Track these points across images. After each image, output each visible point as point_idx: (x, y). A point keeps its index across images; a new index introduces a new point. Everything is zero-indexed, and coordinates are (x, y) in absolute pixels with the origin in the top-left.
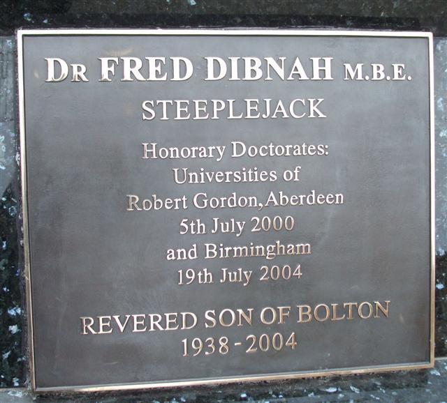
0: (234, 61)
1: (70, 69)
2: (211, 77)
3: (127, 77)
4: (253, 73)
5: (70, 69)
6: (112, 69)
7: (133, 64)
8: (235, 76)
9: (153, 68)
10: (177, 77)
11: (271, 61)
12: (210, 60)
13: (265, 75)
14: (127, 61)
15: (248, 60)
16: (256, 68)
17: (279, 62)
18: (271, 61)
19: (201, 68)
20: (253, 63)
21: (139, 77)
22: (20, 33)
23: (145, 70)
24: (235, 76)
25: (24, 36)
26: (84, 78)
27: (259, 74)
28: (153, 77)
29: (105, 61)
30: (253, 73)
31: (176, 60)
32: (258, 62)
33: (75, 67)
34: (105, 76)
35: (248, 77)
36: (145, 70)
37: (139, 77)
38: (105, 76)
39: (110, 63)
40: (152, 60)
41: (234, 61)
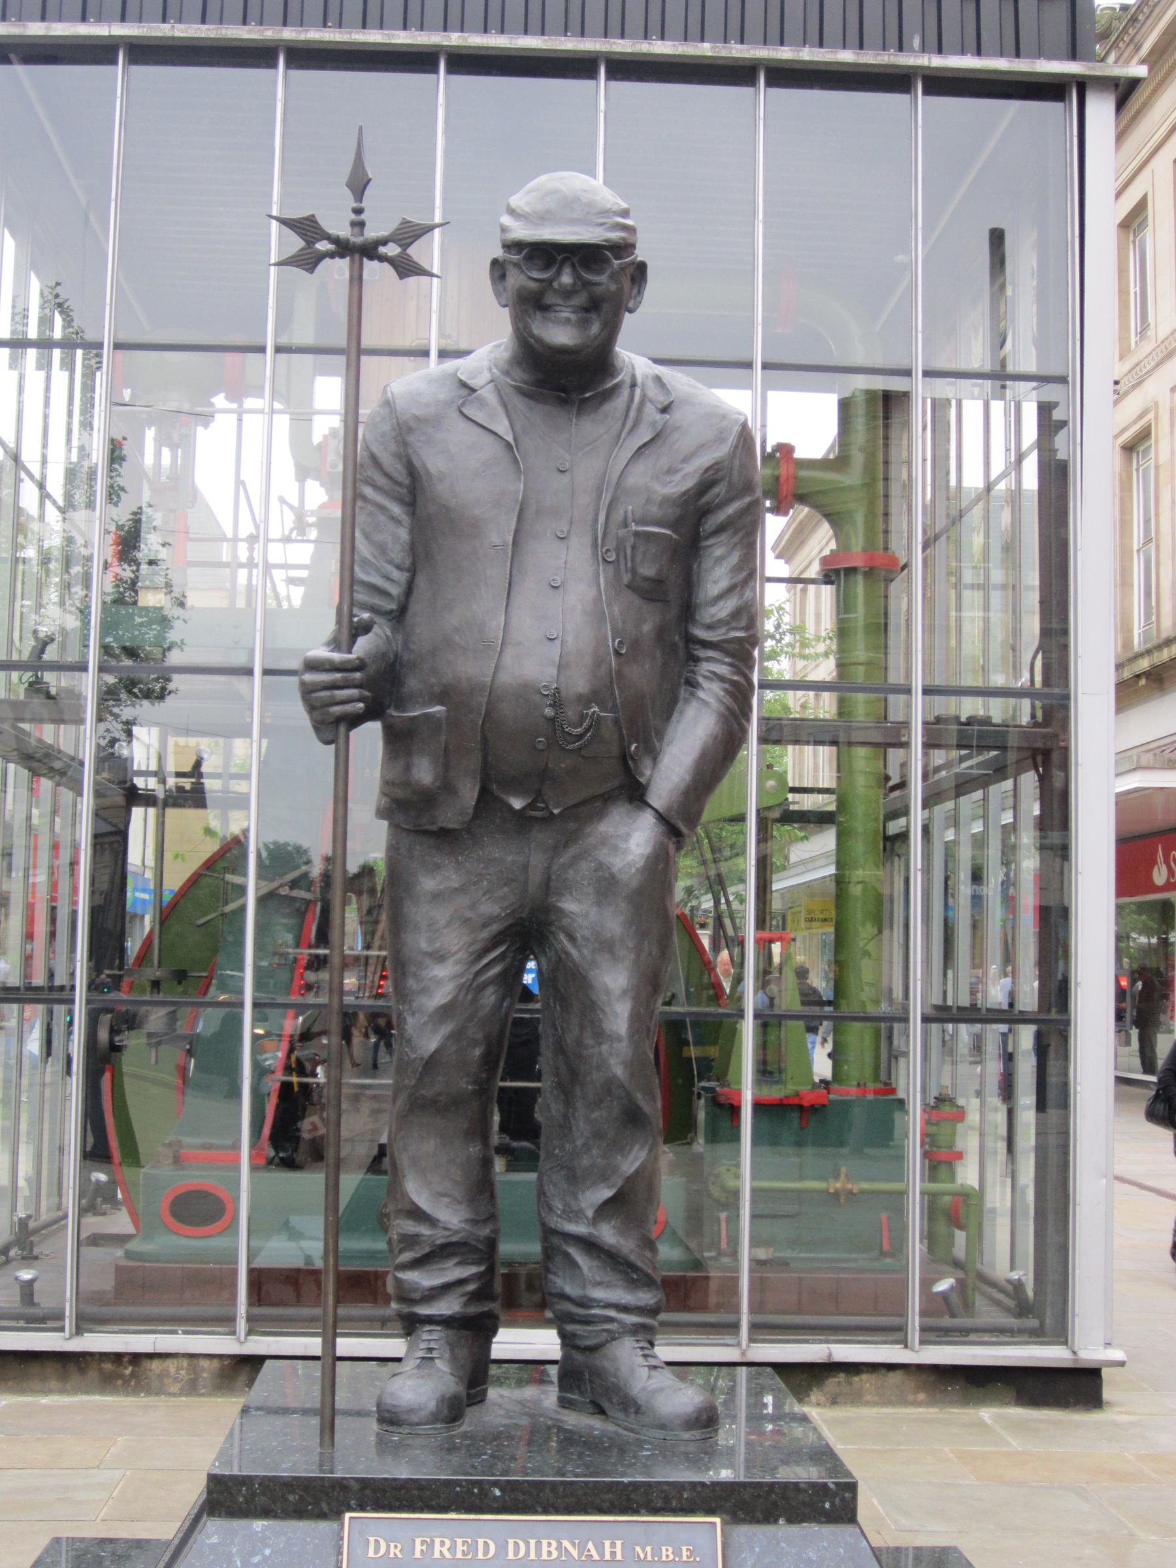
0: (532, 1542)
1: (388, 1547)
2: (511, 1556)
3: (437, 1555)
4: (550, 1553)
5: (388, 1547)
6: (424, 1548)
7: (442, 1544)
8: (532, 1556)
9: (460, 1547)
10: (480, 1556)
11: (566, 1543)
12: (511, 1542)
13: (560, 1555)
14: (437, 1541)
15: (545, 1542)
16: (552, 1549)
17: (573, 1544)
18: (566, 1543)
19: (502, 1547)
20: (549, 1544)
21: (448, 1555)
22: (348, 1515)
23: (452, 1549)
24: (532, 1556)
25: (351, 1518)
26: (399, 1555)
27: (555, 1554)
28: (459, 1555)
29: (418, 1541)
30: (550, 1553)
31: (481, 1542)
32: (554, 1544)
33: (392, 1545)
34: (418, 1555)
35: (545, 1556)
36: (452, 1549)
37: (448, 1555)
38: (418, 1555)
39: (423, 1542)
40: (459, 1541)
41: (532, 1542)
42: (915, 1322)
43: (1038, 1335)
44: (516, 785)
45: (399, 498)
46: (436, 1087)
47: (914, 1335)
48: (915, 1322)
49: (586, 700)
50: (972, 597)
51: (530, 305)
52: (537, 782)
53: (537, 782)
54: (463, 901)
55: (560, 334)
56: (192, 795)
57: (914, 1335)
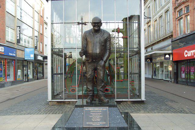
42: (129, 98)
43: (139, 98)
44: (94, 59)
45: (85, 38)
46: (90, 80)
47: (129, 98)
48: (129, 98)
49: (99, 54)
50: (135, 39)
51: (94, 26)
52: (96, 59)
53: (96, 59)
54: (91, 67)
55: (96, 28)
56: (71, 57)
57: (129, 98)
